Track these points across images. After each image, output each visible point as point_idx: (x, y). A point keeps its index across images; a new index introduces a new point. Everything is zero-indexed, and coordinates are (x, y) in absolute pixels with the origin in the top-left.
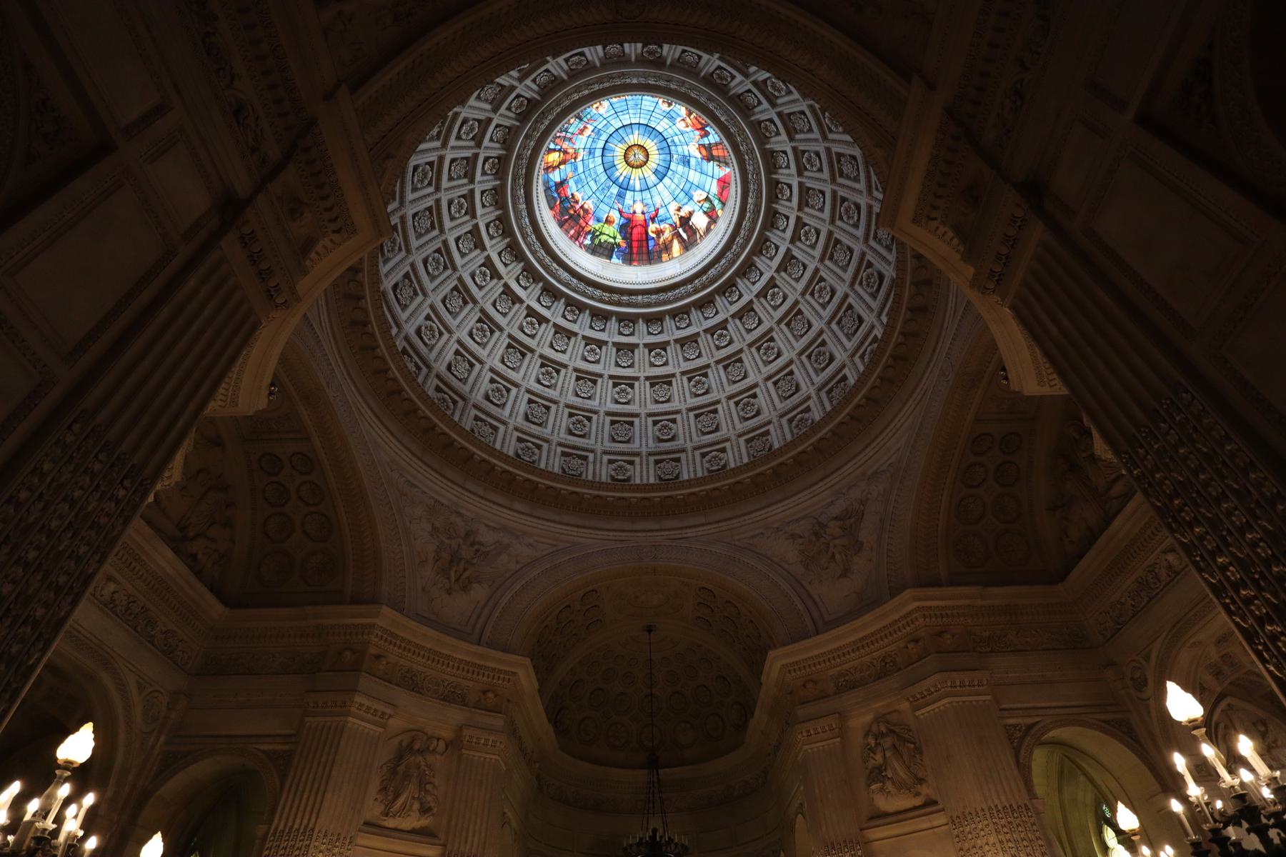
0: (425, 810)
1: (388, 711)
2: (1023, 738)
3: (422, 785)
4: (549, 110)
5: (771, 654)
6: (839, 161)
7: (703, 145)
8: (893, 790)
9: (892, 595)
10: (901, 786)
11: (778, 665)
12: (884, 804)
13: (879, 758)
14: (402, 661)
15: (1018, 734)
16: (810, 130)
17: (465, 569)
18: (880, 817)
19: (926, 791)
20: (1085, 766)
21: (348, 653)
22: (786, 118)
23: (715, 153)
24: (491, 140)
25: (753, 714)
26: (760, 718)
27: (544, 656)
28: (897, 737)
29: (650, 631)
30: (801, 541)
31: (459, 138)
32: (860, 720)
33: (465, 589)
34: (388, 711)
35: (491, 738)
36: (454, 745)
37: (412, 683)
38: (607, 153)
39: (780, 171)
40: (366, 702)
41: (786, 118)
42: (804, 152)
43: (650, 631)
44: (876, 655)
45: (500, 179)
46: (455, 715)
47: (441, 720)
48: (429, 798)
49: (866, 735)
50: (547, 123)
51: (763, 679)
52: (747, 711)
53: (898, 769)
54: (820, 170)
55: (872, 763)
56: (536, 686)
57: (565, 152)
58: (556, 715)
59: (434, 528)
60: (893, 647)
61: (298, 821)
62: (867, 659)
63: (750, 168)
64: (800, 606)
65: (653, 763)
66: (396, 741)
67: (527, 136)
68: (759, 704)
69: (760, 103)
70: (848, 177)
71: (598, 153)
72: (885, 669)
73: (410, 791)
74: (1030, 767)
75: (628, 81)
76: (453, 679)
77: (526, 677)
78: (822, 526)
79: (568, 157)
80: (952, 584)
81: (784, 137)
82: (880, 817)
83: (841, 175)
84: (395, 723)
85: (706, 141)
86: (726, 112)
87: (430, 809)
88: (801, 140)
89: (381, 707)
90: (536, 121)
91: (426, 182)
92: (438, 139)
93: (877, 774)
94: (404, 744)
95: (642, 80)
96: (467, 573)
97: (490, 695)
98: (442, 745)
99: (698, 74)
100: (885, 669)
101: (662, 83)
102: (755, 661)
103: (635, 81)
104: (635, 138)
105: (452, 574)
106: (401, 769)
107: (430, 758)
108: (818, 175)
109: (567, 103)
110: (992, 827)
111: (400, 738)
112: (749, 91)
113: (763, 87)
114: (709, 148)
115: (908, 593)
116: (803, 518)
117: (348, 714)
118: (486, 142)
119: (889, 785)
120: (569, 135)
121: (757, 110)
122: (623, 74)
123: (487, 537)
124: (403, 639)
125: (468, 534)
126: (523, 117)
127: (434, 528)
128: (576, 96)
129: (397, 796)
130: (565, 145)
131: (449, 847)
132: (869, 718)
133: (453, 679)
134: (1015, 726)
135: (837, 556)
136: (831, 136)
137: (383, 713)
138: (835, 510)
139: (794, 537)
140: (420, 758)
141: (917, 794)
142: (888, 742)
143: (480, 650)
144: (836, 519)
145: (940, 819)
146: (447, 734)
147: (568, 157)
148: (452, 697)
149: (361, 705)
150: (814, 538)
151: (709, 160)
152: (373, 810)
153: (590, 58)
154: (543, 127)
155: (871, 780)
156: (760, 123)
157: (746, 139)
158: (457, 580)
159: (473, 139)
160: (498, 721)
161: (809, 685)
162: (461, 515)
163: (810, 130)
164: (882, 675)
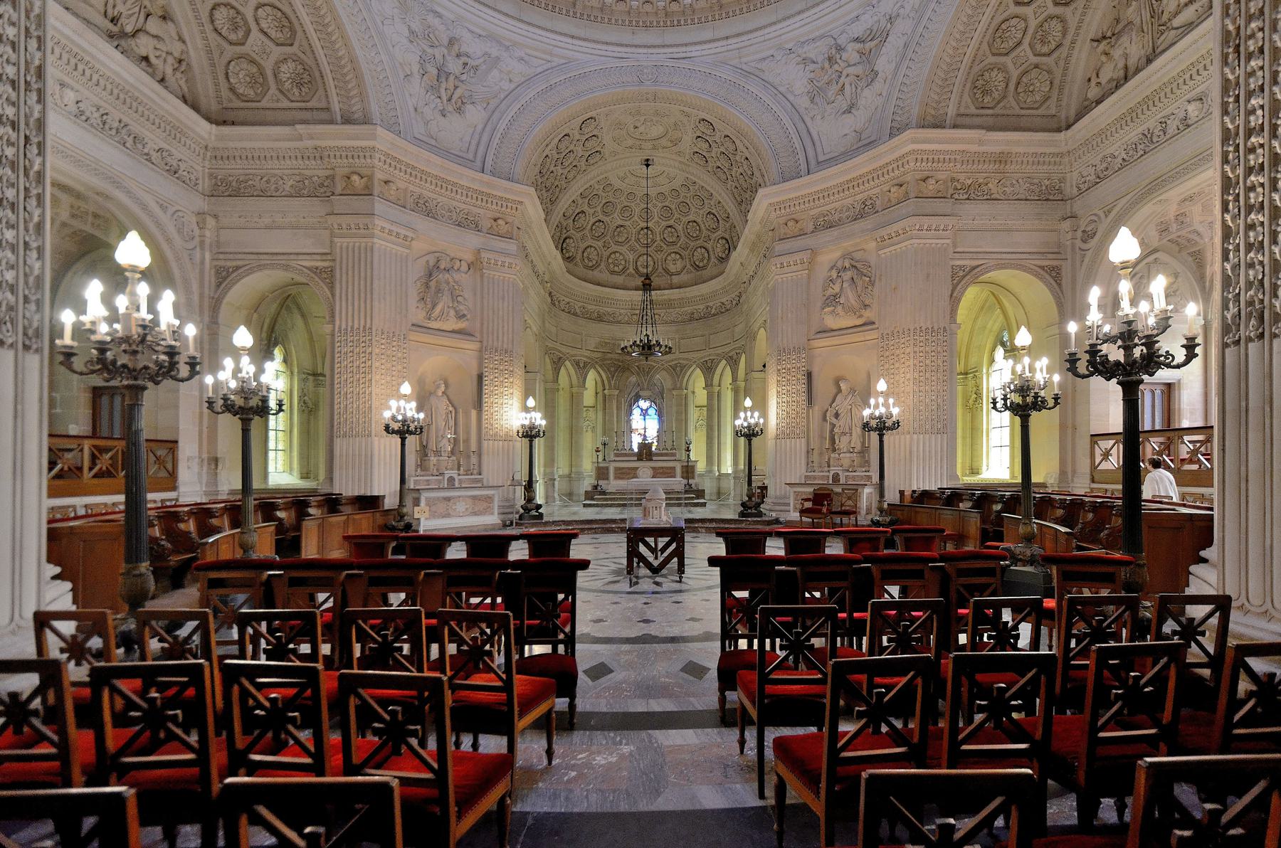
0: (461, 317)
1: (410, 234)
2: (964, 277)
3: (454, 297)
5: (761, 192)
8: (842, 313)
9: (891, 135)
10: (850, 310)
11: (765, 203)
12: (831, 322)
13: (837, 288)
14: (411, 188)
15: (961, 273)
17: (456, 87)
18: (825, 331)
19: (868, 314)
20: (1006, 304)
21: (355, 178)
25: (735, 248)
26: (741, 253)
27: (549, 192)
28: (857, 271)
29: (648, 165)
30: (812, 67)
32: (829, 256)
33: (459, 110)
34: (410, 234)
35: (508, 260)
36: (475, 265)
37: (425, 209)
40: (387, 226)
43: (648, 165)
44: (858, 197)
46: (473, 240)
47: (463, 244)
48: (462, 307)
49: (832, 268)
51: (750, 216)
52: (730, 245)
53: (850, 297)
55: (830, 292)
56: (543, 216)
58: (562, 244)
59: (412, 32)
60: (876, 191)
61: (356, 322)
62: (850, 200)
64: (798, 145)
65: (647, 286)
66: (423, 261)
68: (742, 240)
72: (864, 211)
73: (444, 301)
74: (959, 300)
76: (463, 206)
77: (533, 209)
78: (840, 49)
80: (955, 126)
82: (825, 331)
84: (419, 246)
87: (464, 316)
89: (403, 232)
93: (832, 300)
94: (431, 264)
96: (458, 93)
97: (500, 222)
98: (464, 267)
100: (864, 211)
102: (744, 199)
105: (443, 90)
106: (433, 284)
107: (457, 276)
110: (912, 342)
111: (425, 259)
115: (908, 134)
116: (822, 37)
117: (372, 236)
119: (839, 308)
123: (474, 47)
124: (407, 165)
125: (452, 42)
127: (412, 32)
129: (434, 307)
131: (485, 343)
132: (838, 254)
133: (463, 206)
134: (960, 267)
135: (847, 87)
137: (406, 236)
138: (858, 30)
139: (805, 61)
140: (447, 275)
141: (861, 316)
142: (847, 275)
143: (486, 177)
144: (857, 40)
145: (874, 335)
146: (469, 257)
148: (466, 223)
149: (383, 228)
150: (827, 65)
152: (418, 315)
155: (825, 305)
158: (449, 100)
160: (512, 247)
161: (791, 224)
162: (440, 16)
164: (861, 216)
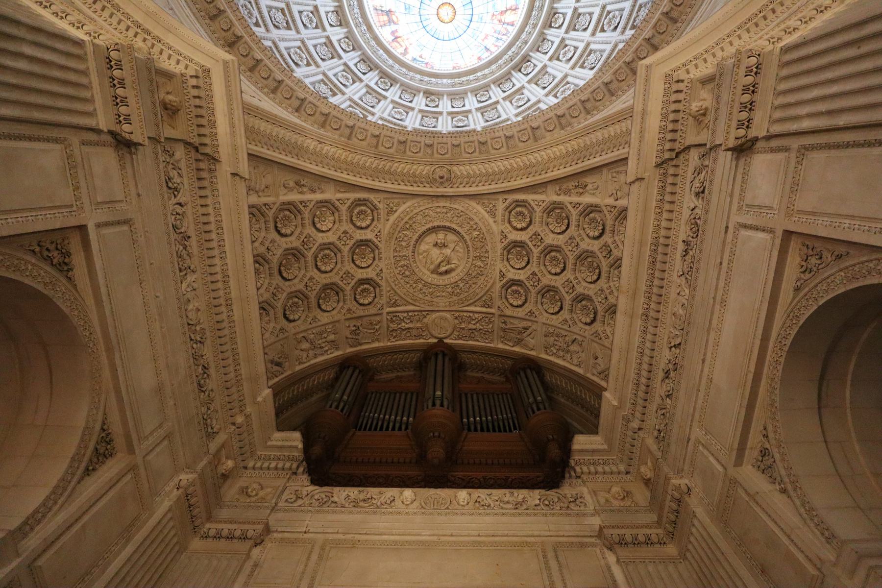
4: (506, 63)
6: (287, 22)
7: (395, 23)
16: (315, 46)
22: (335, 55)
23: (385, 18)
24: (553, 43)
31: (576, 48)
38: (469, 17)
39: (332, 9)
41: (335, 55)
42: (317, 27)
45: (552, 8)
50: (510, 53)
54: (300, 12)
57: (500, 21)
63: (357, 10)
67: (526, 42)
69: (356, 65)
70: (277, 9)
71: (475, 18)
75: (449, 81)
79: (499, 17)
81: (334, 39)
83: (282, 10)
85: (393, 27)
86: (379, 58)
88: (321, 37)
90: (517, 54)
91: (611, 15)
92: (591, 50)
95: (439, 81)
99: (401, 85)
101: (426, 79)
103: (445, 81)
104: (445, 30)
108: (301, 8)
109: (493, 67)
112: (364, 74)
113: (355, 78)
114: (390, 21)
118: (557, 41)
120: (496, 35)
121: (358, 59)
122: (453, 86)
126: (526, 59)
128: (486, 71)
130: (499, 27)
136: (299, 44)
147: (499, 17)
151: (390, 11)
153: (474, 98)
154: (513, 49)
156: (354, 49)
157: (363, 35)
159: (566, 46)
163: (315, 46)
